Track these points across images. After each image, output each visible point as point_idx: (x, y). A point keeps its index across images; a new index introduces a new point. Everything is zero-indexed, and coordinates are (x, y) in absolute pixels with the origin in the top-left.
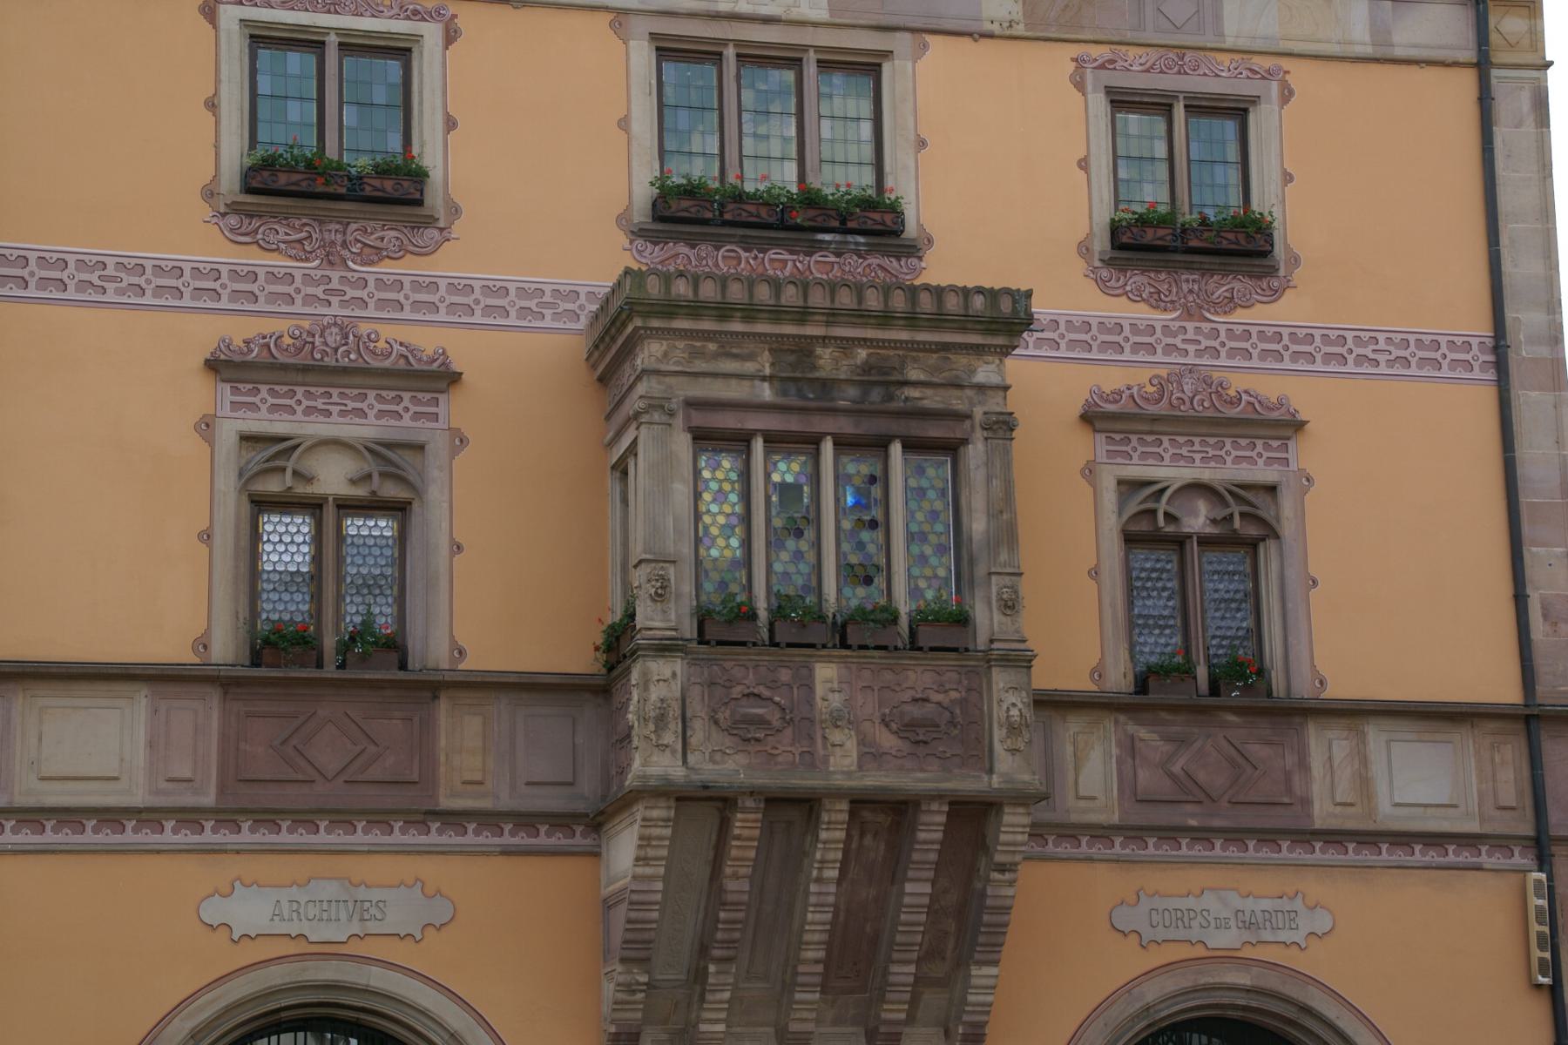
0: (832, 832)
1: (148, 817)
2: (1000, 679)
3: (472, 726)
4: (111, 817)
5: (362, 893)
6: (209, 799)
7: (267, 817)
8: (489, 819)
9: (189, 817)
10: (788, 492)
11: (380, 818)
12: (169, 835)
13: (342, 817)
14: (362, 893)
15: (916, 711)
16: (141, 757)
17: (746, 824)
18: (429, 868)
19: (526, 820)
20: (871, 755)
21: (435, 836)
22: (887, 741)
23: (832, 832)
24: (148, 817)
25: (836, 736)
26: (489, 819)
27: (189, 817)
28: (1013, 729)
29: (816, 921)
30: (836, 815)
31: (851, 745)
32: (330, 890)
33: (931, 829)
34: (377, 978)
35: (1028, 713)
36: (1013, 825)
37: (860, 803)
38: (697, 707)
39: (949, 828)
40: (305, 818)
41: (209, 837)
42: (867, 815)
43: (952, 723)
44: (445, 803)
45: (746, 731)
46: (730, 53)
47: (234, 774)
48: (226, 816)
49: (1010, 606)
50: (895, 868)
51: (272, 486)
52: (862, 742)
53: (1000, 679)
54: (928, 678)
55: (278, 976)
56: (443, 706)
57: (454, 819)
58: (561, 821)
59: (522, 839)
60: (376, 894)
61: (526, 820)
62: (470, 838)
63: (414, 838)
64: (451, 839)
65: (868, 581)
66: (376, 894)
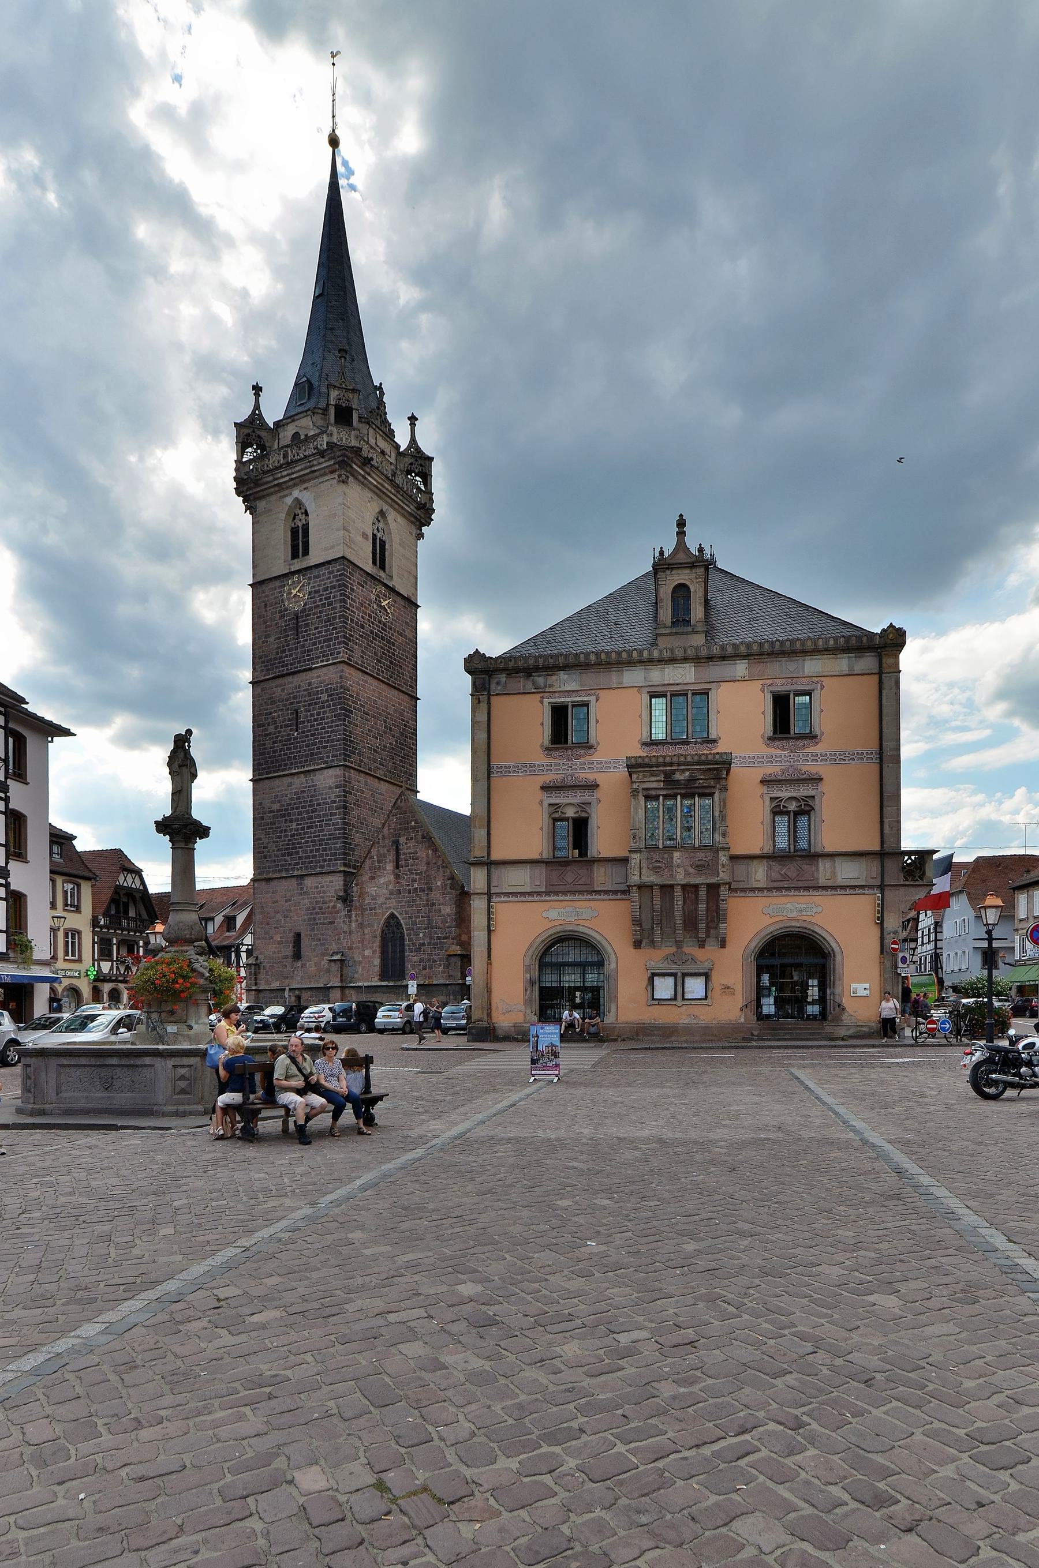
0: (678, 893)
1: (531, 894)
2: (721, 853)
3: (602, 870)
4: (523, 894)
5: (577, 910)
6: (543, 890)
7: (556, 893)
8: (606, 892)
9: (539, 894)
10: (670, 810)
11: (581, 892)
12: (535, 898)
13: (573, 893)
14: (577, 910)
15: (699, 863)
16: (528, 880)
17: (656, 892)
18: (592, 903)
19: (615, 892)
20: (687, 874)
21: (594, 897)
22: (692, 870)
23: (678, 893)
24: (531, 894)
25: (679, 870)
26: (606, 892)
27: (539, 894)
28: (723, 866)
29: (678, 915)
30: (678, 889)
31: (683, 872)
32: (571, 909)
33: (703, 892)
34: (581, 929)
35: (728, 862)
36: (723, 891)
37: (684, 887)
38: (644, 864)
39: (708, 892)
40: (565, 893)
41: (544, 898)
42: (688, 888)
43: (708, 865)
44: (596, 889)
45: (656, 870)
46: (669, 694)
47: (549, 884)
48: (547, 893)
49: (724, 835)
50: (697, 901)
51: (556, 815)
52: (685, 871)
53: (721, 853)
54: (703, 855)
55: (559, 929)
56: (596, 865)
57: (598, 892)
58: (623, 892)
59: (614, 897)
60: (581, 910)
61: (615, 892)
62: (602, 897)
63: (589, 897)
64: (597, 897)
65: (689, 831)
66: (581, 910)
